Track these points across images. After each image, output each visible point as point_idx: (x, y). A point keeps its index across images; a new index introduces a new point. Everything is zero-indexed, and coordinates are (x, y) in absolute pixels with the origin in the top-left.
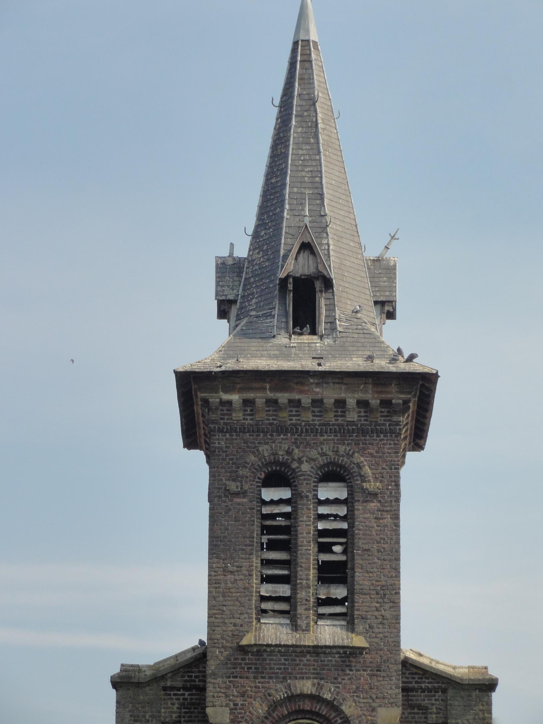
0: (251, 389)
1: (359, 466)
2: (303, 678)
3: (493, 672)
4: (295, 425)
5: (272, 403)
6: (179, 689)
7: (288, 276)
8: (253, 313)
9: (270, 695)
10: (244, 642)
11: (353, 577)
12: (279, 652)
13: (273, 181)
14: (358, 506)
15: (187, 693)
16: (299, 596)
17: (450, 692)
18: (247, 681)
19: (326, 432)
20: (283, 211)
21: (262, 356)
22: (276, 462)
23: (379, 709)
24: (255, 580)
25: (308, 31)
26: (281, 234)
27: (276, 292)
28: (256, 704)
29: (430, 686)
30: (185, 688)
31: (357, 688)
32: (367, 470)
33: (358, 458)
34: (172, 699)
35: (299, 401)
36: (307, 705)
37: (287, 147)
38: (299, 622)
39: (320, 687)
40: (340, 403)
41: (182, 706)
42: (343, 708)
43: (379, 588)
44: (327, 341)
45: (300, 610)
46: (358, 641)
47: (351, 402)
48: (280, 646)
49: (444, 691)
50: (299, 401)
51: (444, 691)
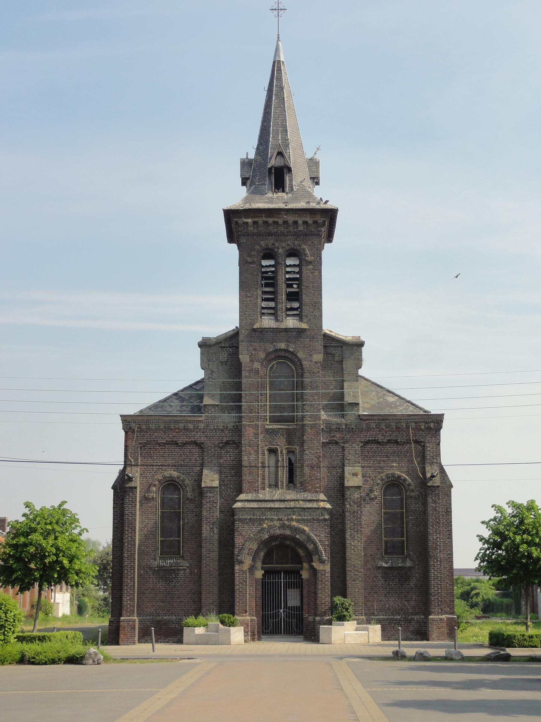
0: (256, 217)
1: (304, 250)
2: (280, 342)
3: (362, 339)
4: (276, 232)
5: (265, 223)
7: (272, 167)
8: (257, 183)
9: (266, 349)
10: (255, 327)
11: (302, 298)
12: (270, 331)
13: (265, 124)
14: (303, 267)
15: (231, 349)
16: (278, 307)
17: (344, 348)
18: (256, 344)
19: (289, 235)
20: (269, 138)
21: (261, 202)
22: (268, 249)
23: (314, 355)
24: (259, 300)
25: (279, 57)
26: (268, 148)
27: (267, 174)
28: (261, 353)
29: (335, 345)
30: (230, 347)
31: (304, 346)
32: (307, 252)
33: (303, 246)
34: (224, 352)
35: (278, 222)
36: (283, 354)
37: (271, 109)
38: (279, 318)
39: (288, 346)
40: (296, 223)
41: (229, 354)
42: (298, 355)
43: (313, 303)
44: (290, 195)
45: (279, 313)
46: (304, 326)
47: (300, 222)
48: (270, 328)
49: (342, 347)
50: (278, 222)
51: (342, 347)
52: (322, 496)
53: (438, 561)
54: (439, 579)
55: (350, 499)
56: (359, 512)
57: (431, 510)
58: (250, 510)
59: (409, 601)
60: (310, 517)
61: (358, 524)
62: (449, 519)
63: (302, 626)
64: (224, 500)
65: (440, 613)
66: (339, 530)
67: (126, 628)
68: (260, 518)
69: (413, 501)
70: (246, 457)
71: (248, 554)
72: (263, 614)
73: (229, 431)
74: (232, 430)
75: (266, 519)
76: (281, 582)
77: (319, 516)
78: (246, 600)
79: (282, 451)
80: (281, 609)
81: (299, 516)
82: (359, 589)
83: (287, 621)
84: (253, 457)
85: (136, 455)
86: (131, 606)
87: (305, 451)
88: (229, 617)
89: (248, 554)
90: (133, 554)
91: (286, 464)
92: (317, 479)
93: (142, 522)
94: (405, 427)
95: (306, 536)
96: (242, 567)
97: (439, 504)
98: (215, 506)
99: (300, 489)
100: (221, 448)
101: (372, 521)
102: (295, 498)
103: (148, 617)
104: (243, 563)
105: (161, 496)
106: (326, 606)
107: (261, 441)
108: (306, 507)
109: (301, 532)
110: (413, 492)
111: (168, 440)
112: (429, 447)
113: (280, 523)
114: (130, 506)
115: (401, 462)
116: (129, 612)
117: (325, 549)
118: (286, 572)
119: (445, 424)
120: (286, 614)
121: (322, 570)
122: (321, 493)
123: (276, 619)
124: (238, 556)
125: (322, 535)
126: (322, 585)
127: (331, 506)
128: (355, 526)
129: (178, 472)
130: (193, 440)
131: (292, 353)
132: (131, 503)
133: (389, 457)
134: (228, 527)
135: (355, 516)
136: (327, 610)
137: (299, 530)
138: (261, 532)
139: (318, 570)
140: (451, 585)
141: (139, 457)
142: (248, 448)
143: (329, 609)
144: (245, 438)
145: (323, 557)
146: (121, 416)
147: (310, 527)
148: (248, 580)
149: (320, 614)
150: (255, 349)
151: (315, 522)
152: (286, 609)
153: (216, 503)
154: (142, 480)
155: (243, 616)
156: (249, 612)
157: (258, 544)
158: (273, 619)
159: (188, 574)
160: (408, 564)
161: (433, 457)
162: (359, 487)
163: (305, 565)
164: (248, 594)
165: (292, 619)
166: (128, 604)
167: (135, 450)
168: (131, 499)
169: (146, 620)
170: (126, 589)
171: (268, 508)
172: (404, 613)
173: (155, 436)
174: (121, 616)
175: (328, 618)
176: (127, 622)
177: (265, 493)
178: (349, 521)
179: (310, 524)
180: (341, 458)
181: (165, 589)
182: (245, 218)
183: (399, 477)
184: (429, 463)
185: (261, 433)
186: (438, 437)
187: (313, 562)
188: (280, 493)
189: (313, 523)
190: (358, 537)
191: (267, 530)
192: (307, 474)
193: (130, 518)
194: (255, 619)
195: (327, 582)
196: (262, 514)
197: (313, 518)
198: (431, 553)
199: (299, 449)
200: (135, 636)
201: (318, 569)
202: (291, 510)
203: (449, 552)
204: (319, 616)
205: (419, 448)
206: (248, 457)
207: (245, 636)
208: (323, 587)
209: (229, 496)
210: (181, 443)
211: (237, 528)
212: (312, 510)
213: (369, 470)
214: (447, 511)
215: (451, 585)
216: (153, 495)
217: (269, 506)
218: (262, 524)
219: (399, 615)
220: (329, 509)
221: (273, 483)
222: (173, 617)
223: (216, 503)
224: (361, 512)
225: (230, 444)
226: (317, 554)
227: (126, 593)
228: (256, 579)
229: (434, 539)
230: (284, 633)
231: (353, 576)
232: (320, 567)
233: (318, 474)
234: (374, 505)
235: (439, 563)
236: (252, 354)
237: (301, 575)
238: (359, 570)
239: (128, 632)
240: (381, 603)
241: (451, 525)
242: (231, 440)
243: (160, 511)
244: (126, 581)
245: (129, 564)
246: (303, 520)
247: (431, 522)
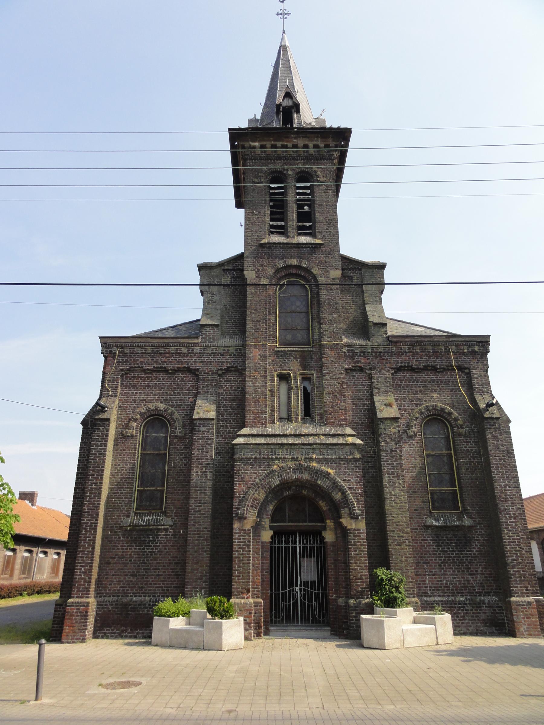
0: (264, 141)
1: (316, 172)
4: (285, 157)
6: (231, 270)
9: (276, 265)
11: (315, 217)
12: (280, 247)
17: (363, 270)
18: (264, 260)
23: (330, 271)
24: (267, 218)
30: (234, 270)
31: (319, 262)
33: (314, 168)
35: (287, 145)
36: (294, 271)
39: (301, 262)
40: (306, 146)
41: (232, 278)
42: (312, 271)
47: (311, 145)
49: (360, 270)
50: (287, 145)
51: (360, 270)
52: (349, 431)
53: (512, 517)
54: (517, 543)
55: (384, 434)
56: (398, 451)
57: (493, 449)
58: (255, 446)
59: (474, 574)
60: (335, 457)
61: (398, 466)
62: (512, 462)
63: (327, 611)
64: (223, 438)
65: (525, 593)
66: (372, 477)
67: (74, 615)
68: (268, 458)
69: (462, 440)
70: (250, 383)
71: (252, 506)
72: (271, 594)
73: (230, 355)
74: (234, 355)
75: (276, 458)
76: (296, 547)
77: (348, 455)
78: (249, 573)
79: (295, 377)
80: (297, 586)
81: (321, 455)
82: (407, 557)
83: (305, 603)
84: (259, 383)
85: (115, 383)
86: (85, 581)
87: (325, 376)
88: (221, 601)
89: (252, 506)
90: (95, 507)
91: (301, 392)
92: (341, 409)
93: (114, 466)
94: (444, 351)
95: (330, 481)
96: (243, 525)
97: (501, 441)
98: (209, 442)
99: (320, 423)
100: (220, 375)
101: (412, 464)
102: (314, 432)
103: (111, 599)
104: (245, 518)
105: (143, 434)
106: (363, 582)
107: (269, 366)
108: (329, 442)
109: (324, 476)
110: (462, 428)
111: (156, 366)
112: (476, 374)
113: (295, 464)
114: (99, 443)
115: (442, 393)
116: (81, 591)
117: (357, 499)
118: (304, 533)
119: (492, 347)
120: (304, 594)
121: (355, 530)
122: (347, 426)
123: (290, 601)
124: (239, 509)
125: (352, 480)
126: (355, 551)
127: (362, 440)
128: (394, 469)
129: (166, 405)
130: (187, 366)
131: (306, 270)
132: (100, 440)
133: (427, 387)
134: (226, 472)
135: (393, 457)
136: (365, 588)
137: (321, 474)
138: (270, 476)
139: (349, 530)
140: (528, 552)
141: (119, 386)
142: (254, 372)
143: (368, 588)
144: (249, 360)
145: (355, 510)
146: (100, 338)
147: (336, 469)
148: (251, 543)
149: (355, 595)
150: (262, 265)
151: (342, 462)
152: (304, 586)
153: (210, 439)
154: (121, 414)
155: (243, 598)
156: (252, 591)
157: (265, 492)
158: (286, 602)
159: (171, 536)
160: (467, 522)
161: (482, 385)
162: (395, 419)
163: (329, 523)
164: (251, 565)
165: (312, 602)
166: (82, 579)
167: (114, 378)
168: (101, 435)
169: (108, 603)
170: (81, 557)
171: (279, 444)
172: (468, 593)
173: (141, 362)
174: (70, 597)
175: (367, 601)
176: (76, 606)
177: (274, 427)
178: (385, 463)
179: (335, 465)
180: (367, 387)
181: (139, 557)
182: (253, 141)
183: (442, 410)
184: (479, 392)
185: (269, 356)
186: (485, 362)
187: (341, 518)
188: (294, 427)
189: (340, 464)
190: (400, 484)
191: (278, 473)
192: (328, 403)
193: (97, 459)
194: (261, 603)
195: (362, 547)
196: (272, 452)
197: (340, 458)
198: (500, 506)
199: (317, 375)
200: (86, 629)
201: (349, 527)
202: (309, 447)
203: (518, 506)
204: (353, 598)
205: (463, 376)
206: (253, 383)
207: (246, 630)
208: (357, 554)
209: (229, 433)
210: (171, 370)
211: (238, 471)
212: (337, 447)
213: (404, 401)
214: (509, 453)
215: (528, 552)
216: (133, 432)
217: (280, 442)
218: (271, 465)
219: (462, 596)
220: (360, 445)
221: (284, 415)
222: (147, 598)
223: (210, 439)
224: (401, 451)
225: (231, 371)
226: (346, 507)
227: (80, 563)
228: (262, 543)
229: (501, 487)
230: (301, 623)
231: (397, 538)
232: (351, 524)
233: (342, 404)
234: (413, 445)
235: (513, 520)
236: (258, 270)
237: (324, 538)
239: (77, 622)
240: (436, 578)
241: (517, 470)
242: (232, 367)
243: (140, 452)
244: (82, 546)
245: (89, 520)
246: (326, 459)
247: (494, 464)
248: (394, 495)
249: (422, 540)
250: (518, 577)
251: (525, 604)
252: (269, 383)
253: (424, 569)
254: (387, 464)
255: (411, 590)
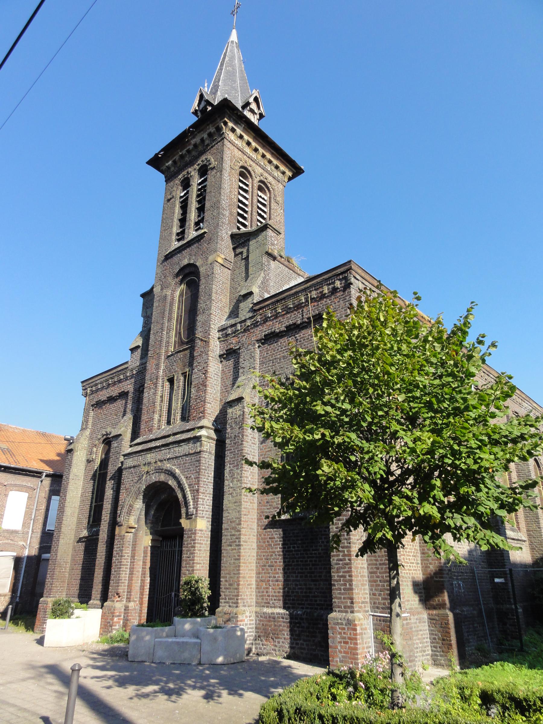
36: (187, 271)
59: (317, 581)
65: (349, 607)
101: (269, 448)
117: (194, 496)
128: (235, 457)
145: (190, 508)
172: (309, 604)
219: (303, 608)
238: (236, 528)
248: (232, 488)
249: (270, 538)
250: (342, 585)
251: (344, 623)
252: (160, 388)
253: (269, 573)
254: (230, 453)
255: (236, 598)
